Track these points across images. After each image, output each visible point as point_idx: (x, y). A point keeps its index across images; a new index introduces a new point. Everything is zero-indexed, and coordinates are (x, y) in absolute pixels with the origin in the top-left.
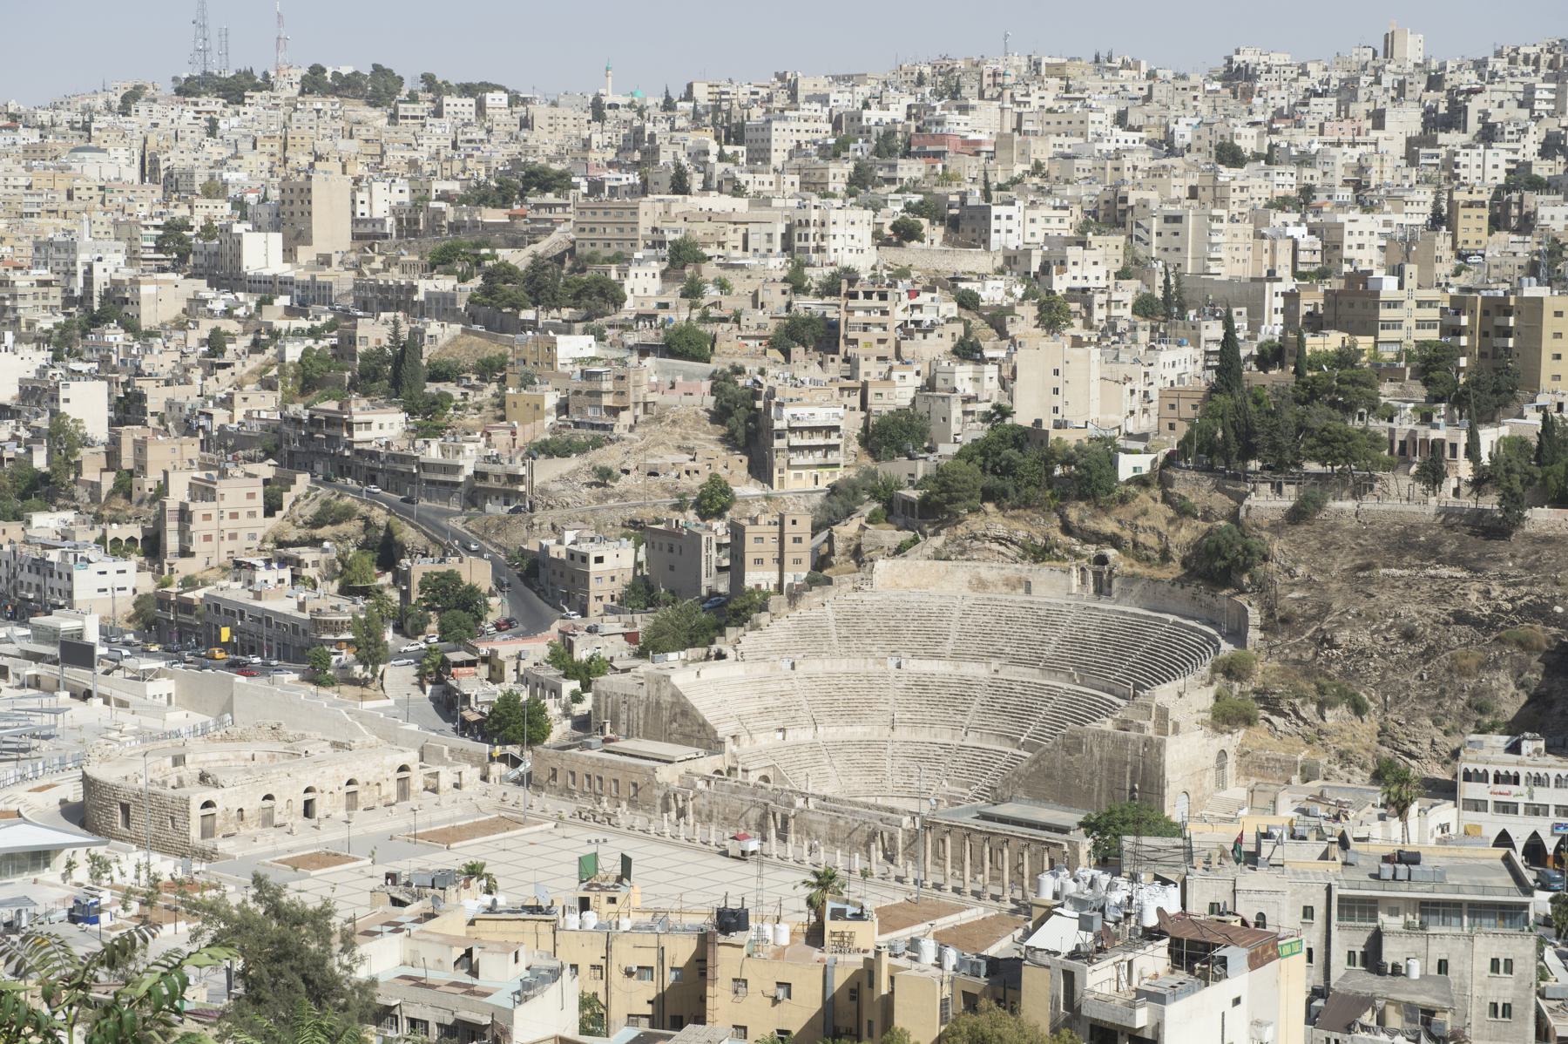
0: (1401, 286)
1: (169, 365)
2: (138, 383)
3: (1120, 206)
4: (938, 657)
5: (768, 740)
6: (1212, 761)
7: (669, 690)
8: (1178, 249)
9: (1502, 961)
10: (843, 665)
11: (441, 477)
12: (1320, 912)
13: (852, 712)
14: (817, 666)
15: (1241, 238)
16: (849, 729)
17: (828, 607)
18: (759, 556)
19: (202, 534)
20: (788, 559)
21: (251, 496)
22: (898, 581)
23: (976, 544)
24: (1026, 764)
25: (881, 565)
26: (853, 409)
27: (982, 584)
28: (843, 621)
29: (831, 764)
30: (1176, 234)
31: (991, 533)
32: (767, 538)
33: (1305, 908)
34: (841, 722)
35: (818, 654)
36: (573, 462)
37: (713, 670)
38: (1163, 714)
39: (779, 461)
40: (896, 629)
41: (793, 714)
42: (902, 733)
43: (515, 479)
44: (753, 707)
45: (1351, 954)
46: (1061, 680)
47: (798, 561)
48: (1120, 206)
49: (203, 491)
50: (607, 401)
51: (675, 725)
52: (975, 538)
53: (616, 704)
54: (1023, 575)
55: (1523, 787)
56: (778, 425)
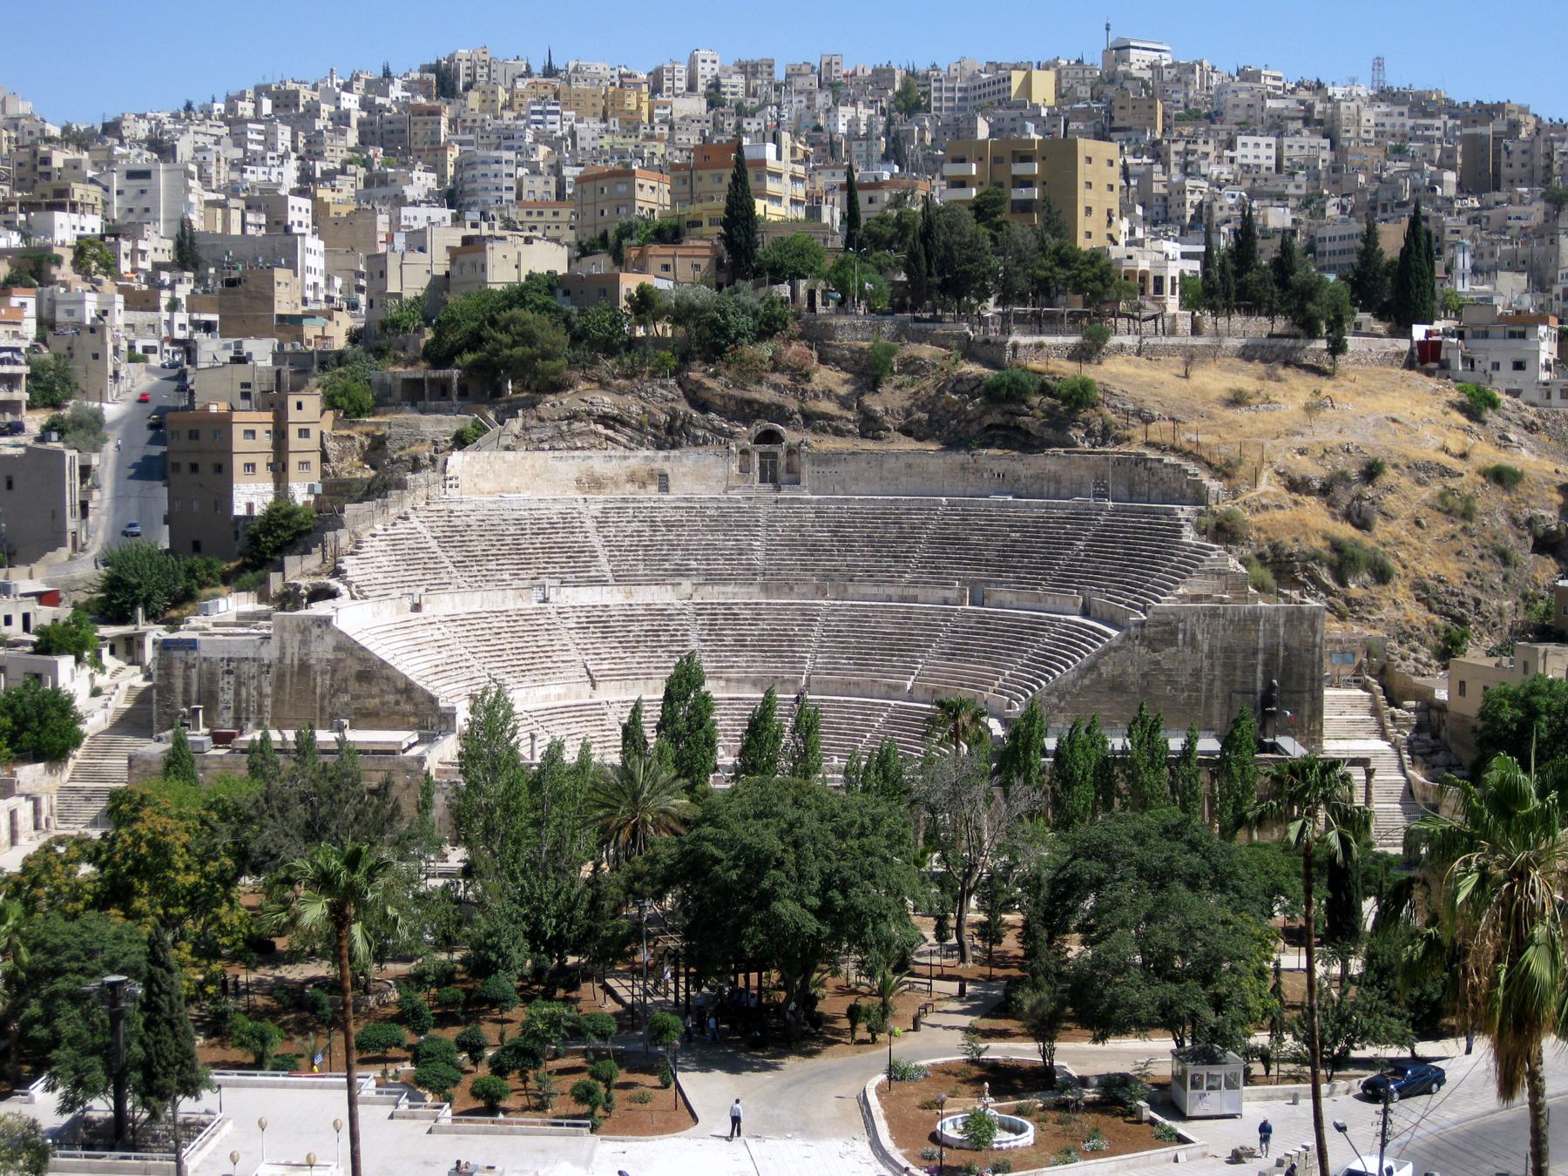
3: (41, 169)
7: (330, 641)
16: (541, 691)
17: (415, 521)
18: (250, 459)
20: (293, 461)
23: (577, 426)
27: (596, 483)
28: (445, 541)
32: (260, 431)
34: (527, 681)
40: (518, 549)
46: (804, 596)
47: (305, 464)
48: (41, 169)
51: (346, 698)
54: (656, 466)
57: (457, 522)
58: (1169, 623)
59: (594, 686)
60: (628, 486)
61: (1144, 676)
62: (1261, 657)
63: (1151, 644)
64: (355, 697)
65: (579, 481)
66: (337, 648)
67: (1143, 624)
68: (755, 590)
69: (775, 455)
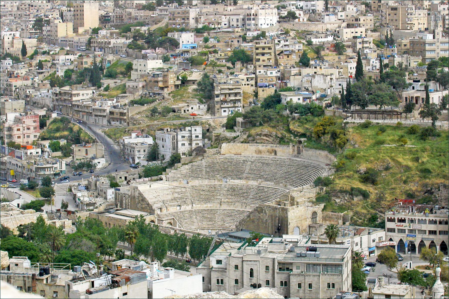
0: (434, 38)
1: (24, 73)
2: (10, 80)
4: (240, 178)
5: (173, 209)
6: (310, 216)
8: (396, 20)
9: (331, 284)
10: (206, 182)
11: (99, 114)
12: (271, 268)
13: (207, 200)
14: (196, 183)
15: (422, 15)
16: (205, 205)
19: (17, 136)
21: (35, 122)
22: (231, 151)
24: (246, 218)
25: (224, 145)
26: (252, 85)
29: (196, 218)
30: (395, 14)
31: (264, 133)
33: (266, 266)
34: (202, 203)
35: (197, 178)
36: (146, 107)
37: (156, 185)
38: (293, 199)
39: (217, 106)
41: (184, 200)
42: (224, 207)
43: (122, 114)
44: (170, 197)
45: (282, 282)
48: (379, 4)
49: (18, 121)
50: (161, 84)
52: (257, 135)
53: (122, 197)
54: (274, 148)
55: (407, 224)
56: (216, 92)
57: (215, 161)
58: (261, 208)
59: (221, 205)
60: (268, 153)
61: (258, 219)
62: (277, 218)
63: (259, 212)
64: (142, 205)
65: (256, 151)
66: (139, 194)
67: (257, 207)
68: (273, 183)
69: (299, 147)
